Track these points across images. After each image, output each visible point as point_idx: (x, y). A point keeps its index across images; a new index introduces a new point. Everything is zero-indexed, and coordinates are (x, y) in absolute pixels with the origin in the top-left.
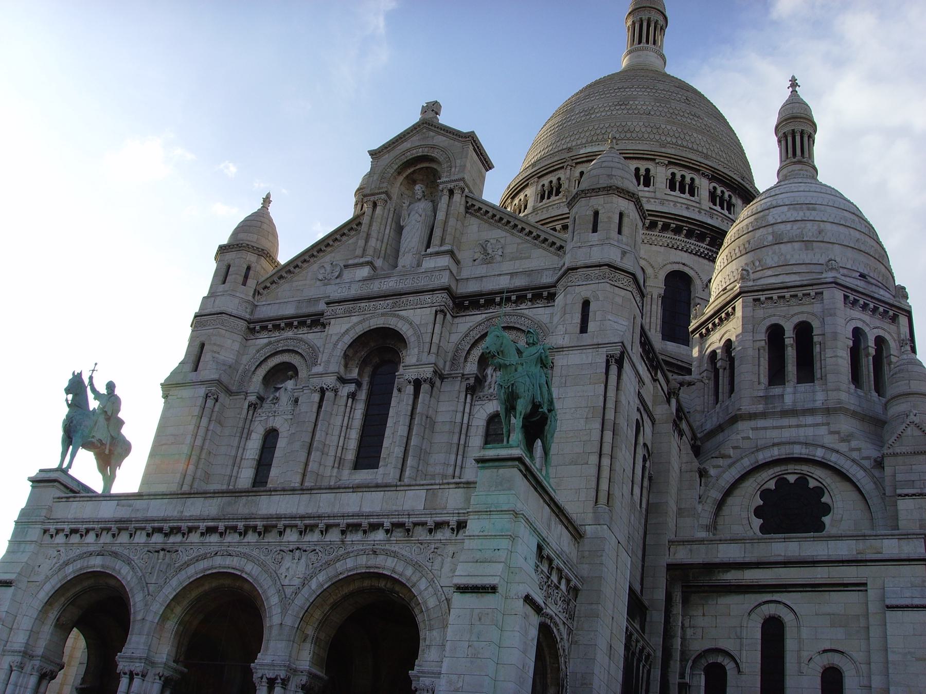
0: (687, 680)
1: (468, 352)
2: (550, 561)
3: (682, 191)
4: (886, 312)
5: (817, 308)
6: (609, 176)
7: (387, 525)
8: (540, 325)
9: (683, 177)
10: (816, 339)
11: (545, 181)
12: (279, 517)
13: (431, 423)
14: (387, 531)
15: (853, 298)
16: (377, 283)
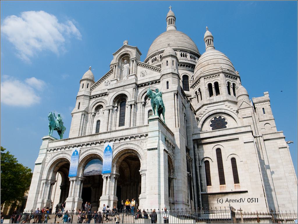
0: (201, 165)
1: (142, 97)
2: (168, 141)
3: (184, 57)
4: (234, 77)
5: (219, 78)
7: (129, 137)
9: (184, 53)
10: (219, 85)
11: (153, 58)
12: (104, 139)
13: (135, 114)
14: (130, 139)
15: (227, 75)
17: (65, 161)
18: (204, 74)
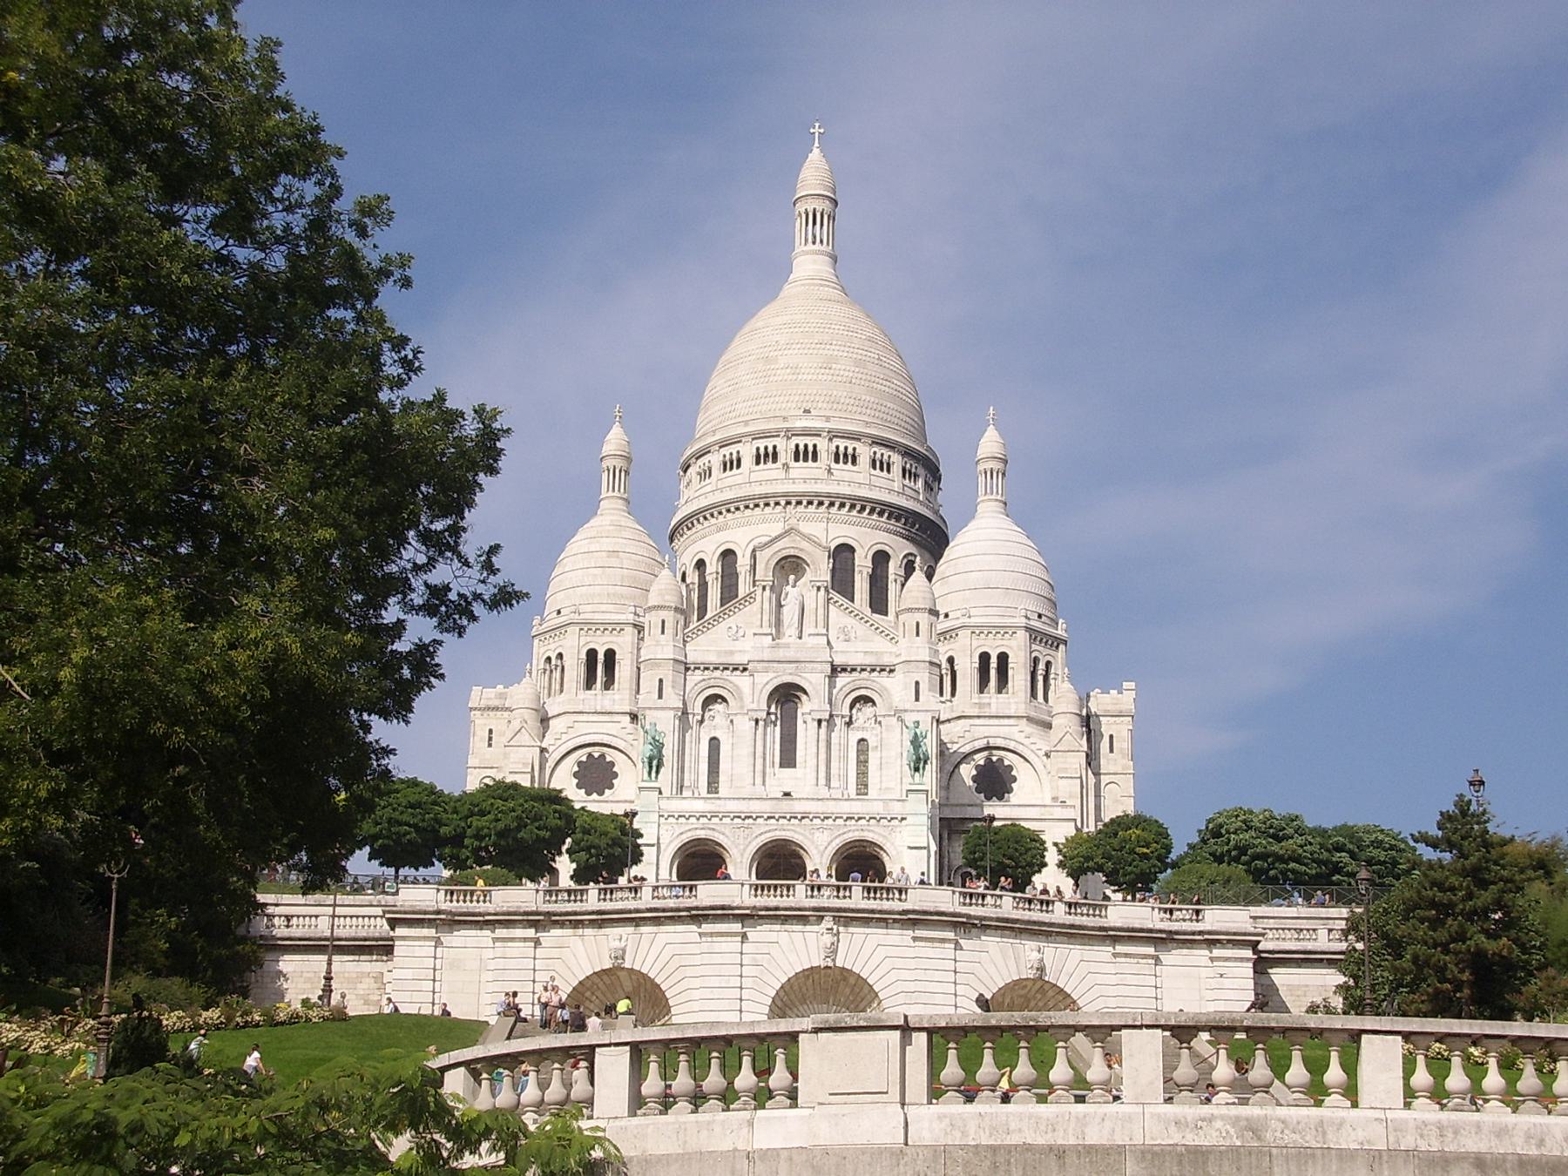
5: (1013, 643)
6: (924, 598)
7: (867, 818)
8: (886, 689)
9: (882, 455)
10: (1010, 666)
11: (761, 444)
15: (1035, 635)
16: (781, 650)
17: (707, 845)
18: (973, 621)
